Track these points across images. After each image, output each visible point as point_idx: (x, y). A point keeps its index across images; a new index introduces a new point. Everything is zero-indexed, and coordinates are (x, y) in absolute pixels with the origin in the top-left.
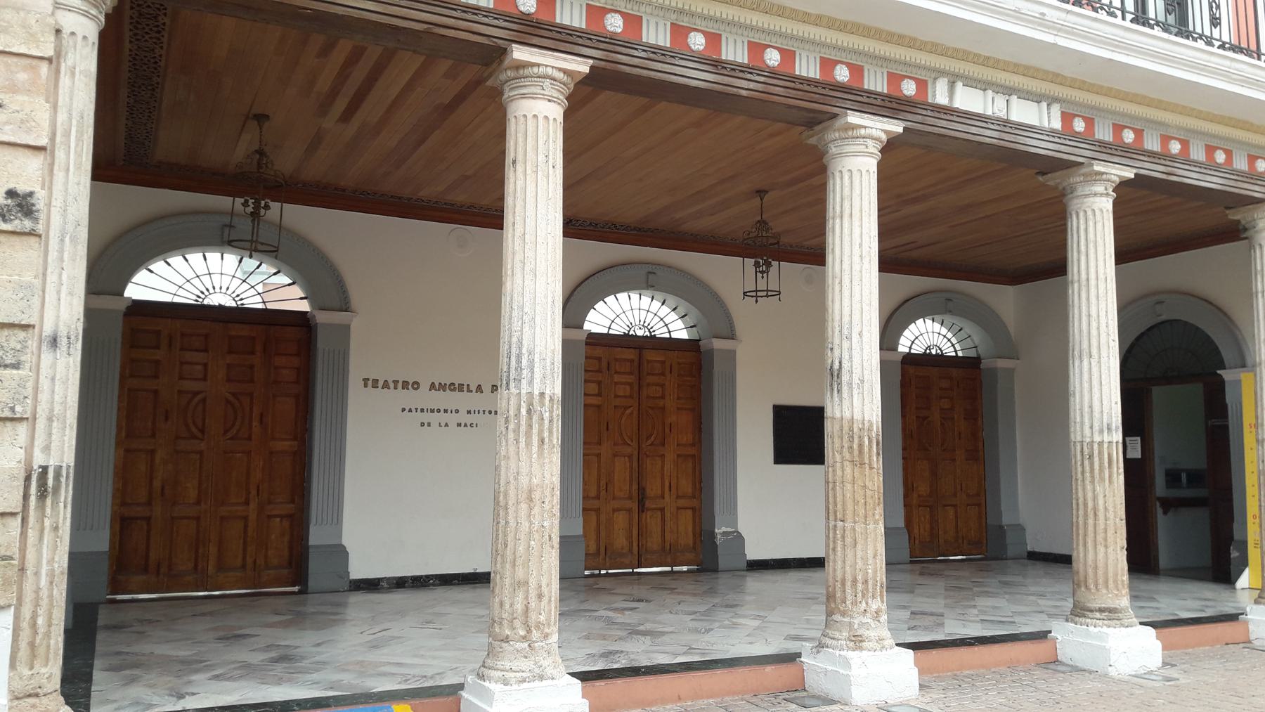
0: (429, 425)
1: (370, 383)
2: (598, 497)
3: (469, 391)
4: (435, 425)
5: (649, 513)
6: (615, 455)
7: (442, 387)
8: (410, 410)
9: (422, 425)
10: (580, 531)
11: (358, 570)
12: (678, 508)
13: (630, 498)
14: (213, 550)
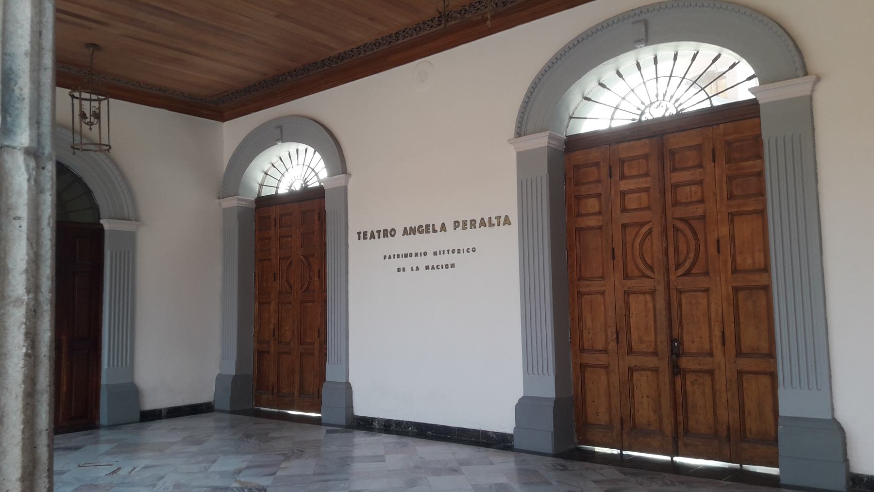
0: (404, 270)
1: (362, 235)
2: (605, 351)
3: (435, 231)
4: (408, 269)
5: (690, 378)
6: (627, 294)
7: (413, 231)
8: (390, 257)
9: (399, 270)
10: (551, 394)
11: (361, 409)
12: (740, 373)
13: (655, 353)
14: (297, 378)
